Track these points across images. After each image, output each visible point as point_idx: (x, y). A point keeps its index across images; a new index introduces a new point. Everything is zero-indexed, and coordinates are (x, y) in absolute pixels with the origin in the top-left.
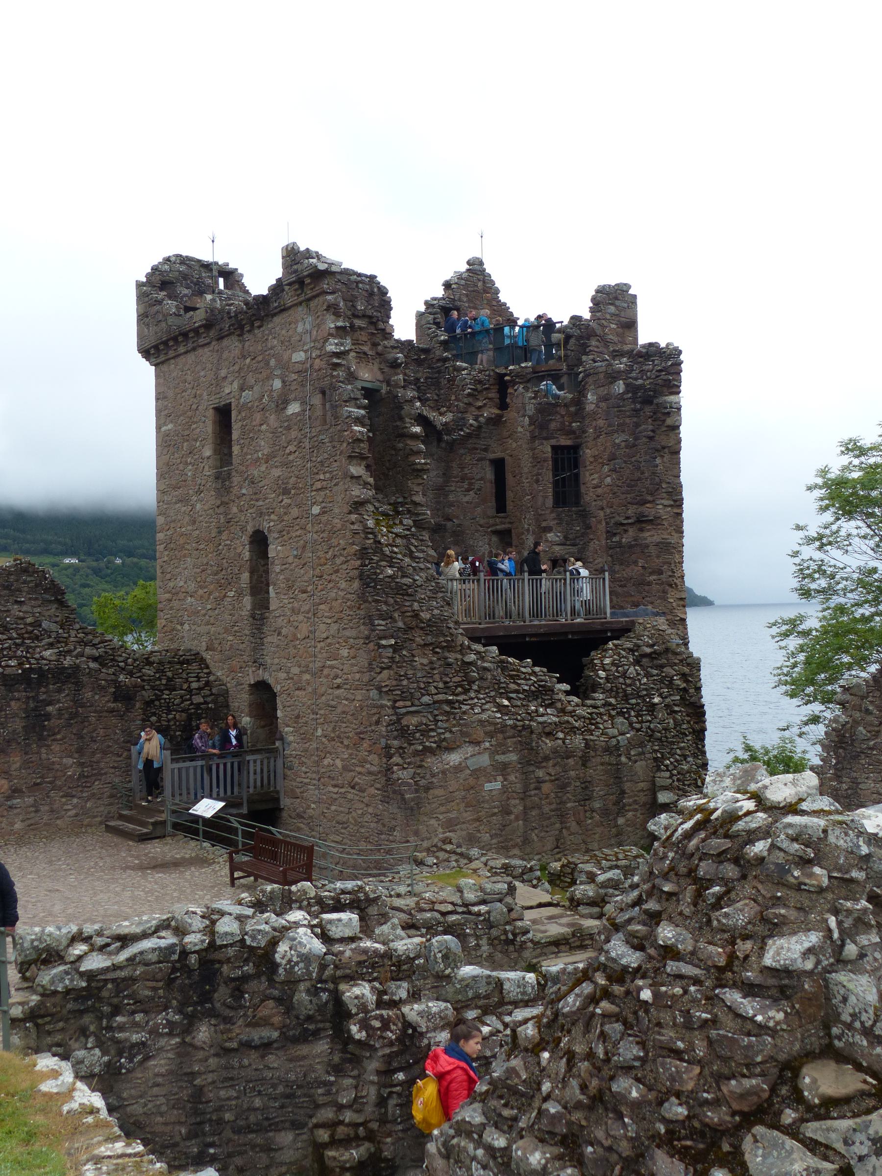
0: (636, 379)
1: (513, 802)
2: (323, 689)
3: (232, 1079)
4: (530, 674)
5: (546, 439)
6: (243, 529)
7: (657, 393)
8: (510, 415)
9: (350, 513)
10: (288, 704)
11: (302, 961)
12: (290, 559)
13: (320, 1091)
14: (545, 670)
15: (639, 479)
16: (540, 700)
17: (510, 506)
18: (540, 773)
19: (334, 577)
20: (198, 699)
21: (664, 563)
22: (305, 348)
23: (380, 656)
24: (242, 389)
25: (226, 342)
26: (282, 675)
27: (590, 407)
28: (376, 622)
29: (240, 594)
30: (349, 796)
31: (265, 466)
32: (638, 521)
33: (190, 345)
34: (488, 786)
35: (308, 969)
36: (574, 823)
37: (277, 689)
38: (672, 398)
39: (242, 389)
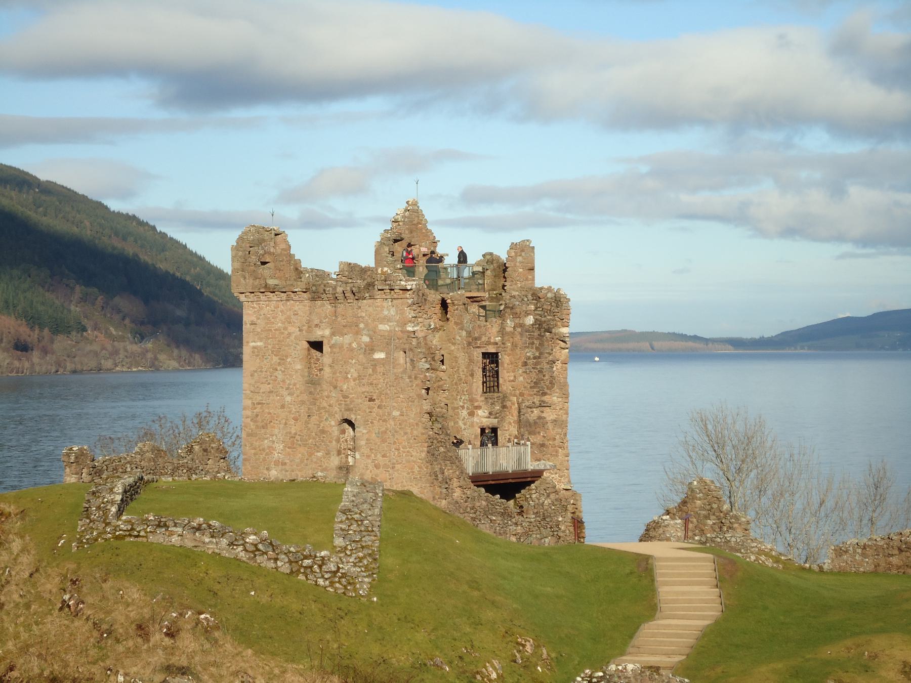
24: (333, 334)
25: (319, 303)
27: (508, 329)
39: (333, 334)
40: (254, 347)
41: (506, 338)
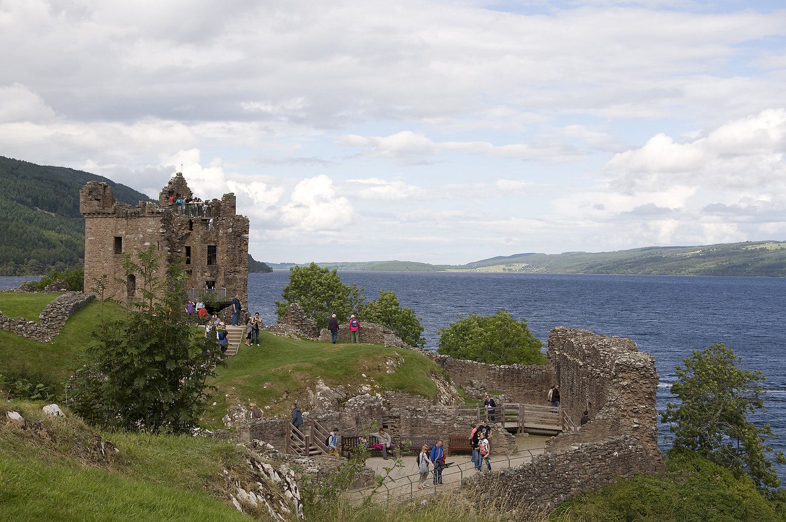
7: (241, 234)
8: (194, 233)
27: (220, 235)
29: (123, 291)
38: (246, 235)
40: (90, 240)
41: (219, 239)
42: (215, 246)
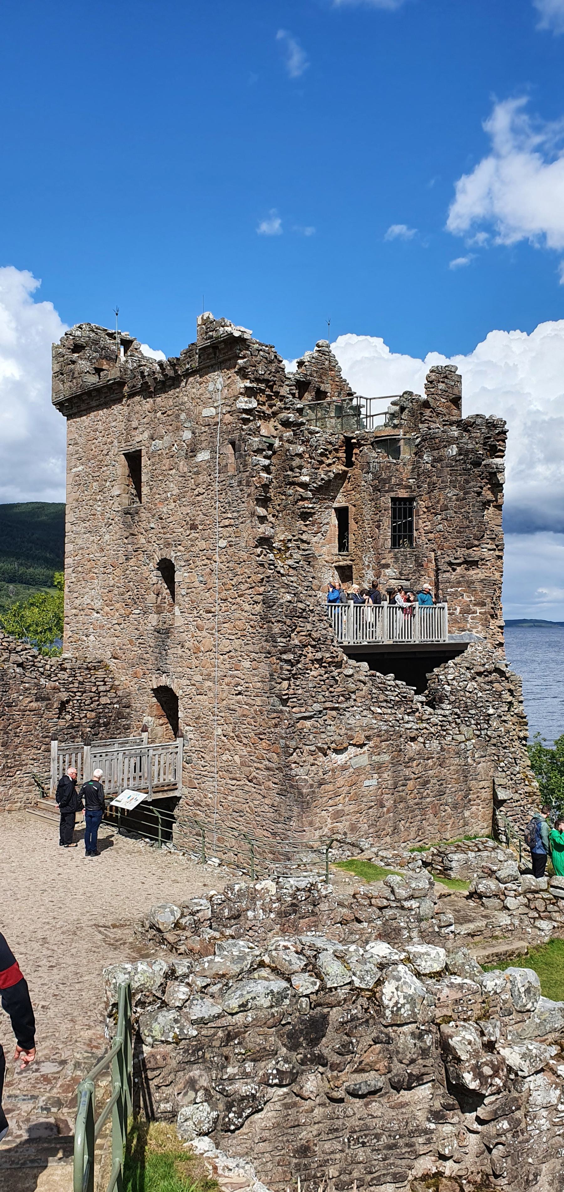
0: (467, 444)
1: (386, 796)
2: (225, 695)
3: (337, 1130)
4: (394, 687)
5: (387, 492)
6: (150, 557)
9: (256, 547)
10: (189, 706)
11: (408, 1003)
12: (197, 584)
13: (421, 1140)
14: (404, 683)
15: (468, 527)
16: (403, 709)
17: (351, 546)
18: (407, 772)
19: (238, 599)
20: (104, 700)
21: (487, 597)
22: (215, 405)
23: (281, 668)
24: (152, 438)
26: (185, 682)
28: (279, 640)
30: (246, 788)
31: (174, 504)
32: (466, 562)
33: (103, 400)
34: (367, 783)
35: (413, 1011)
36: (432, 815)
37: (179, 693)
39: (152, 438)
42: (411, 500)
